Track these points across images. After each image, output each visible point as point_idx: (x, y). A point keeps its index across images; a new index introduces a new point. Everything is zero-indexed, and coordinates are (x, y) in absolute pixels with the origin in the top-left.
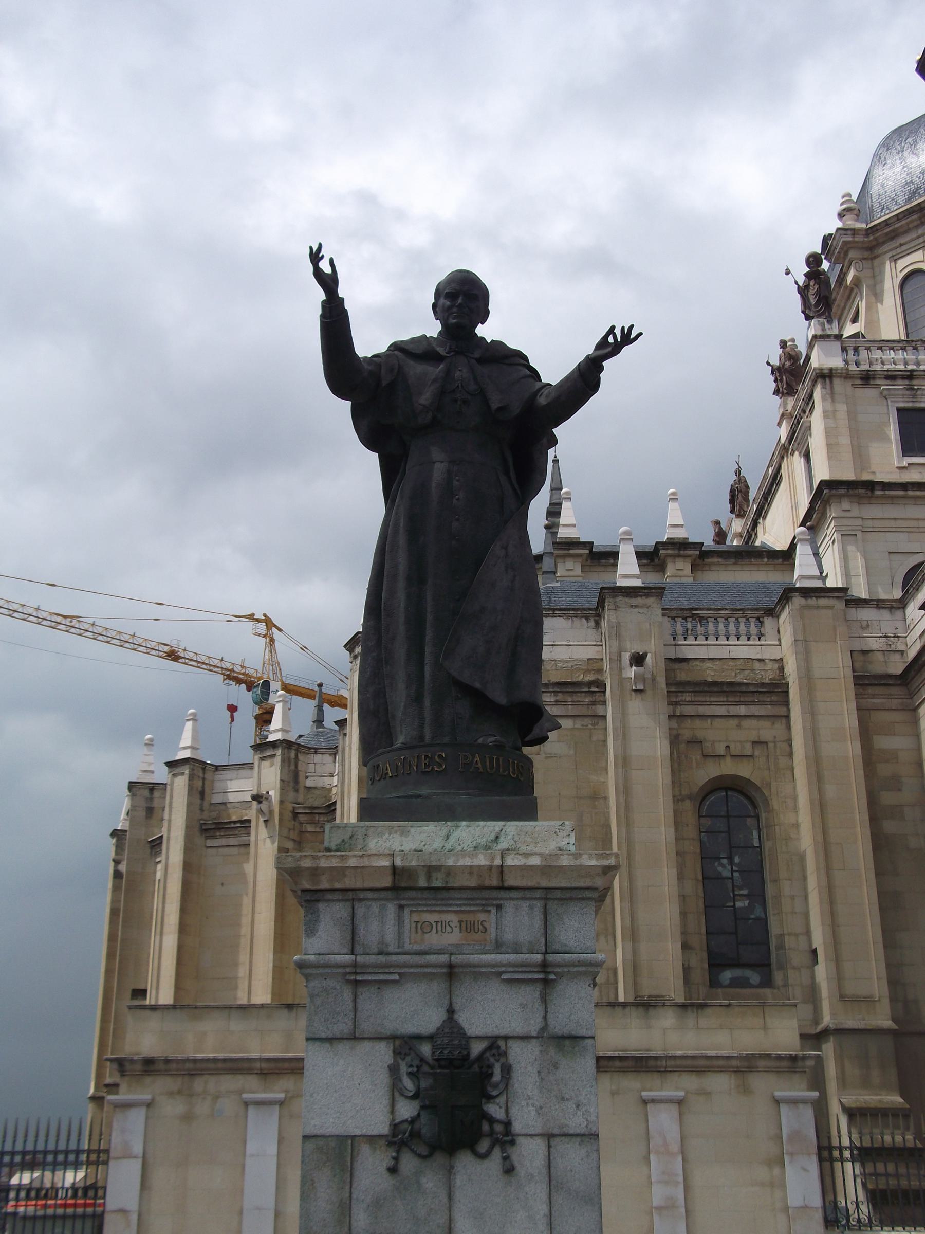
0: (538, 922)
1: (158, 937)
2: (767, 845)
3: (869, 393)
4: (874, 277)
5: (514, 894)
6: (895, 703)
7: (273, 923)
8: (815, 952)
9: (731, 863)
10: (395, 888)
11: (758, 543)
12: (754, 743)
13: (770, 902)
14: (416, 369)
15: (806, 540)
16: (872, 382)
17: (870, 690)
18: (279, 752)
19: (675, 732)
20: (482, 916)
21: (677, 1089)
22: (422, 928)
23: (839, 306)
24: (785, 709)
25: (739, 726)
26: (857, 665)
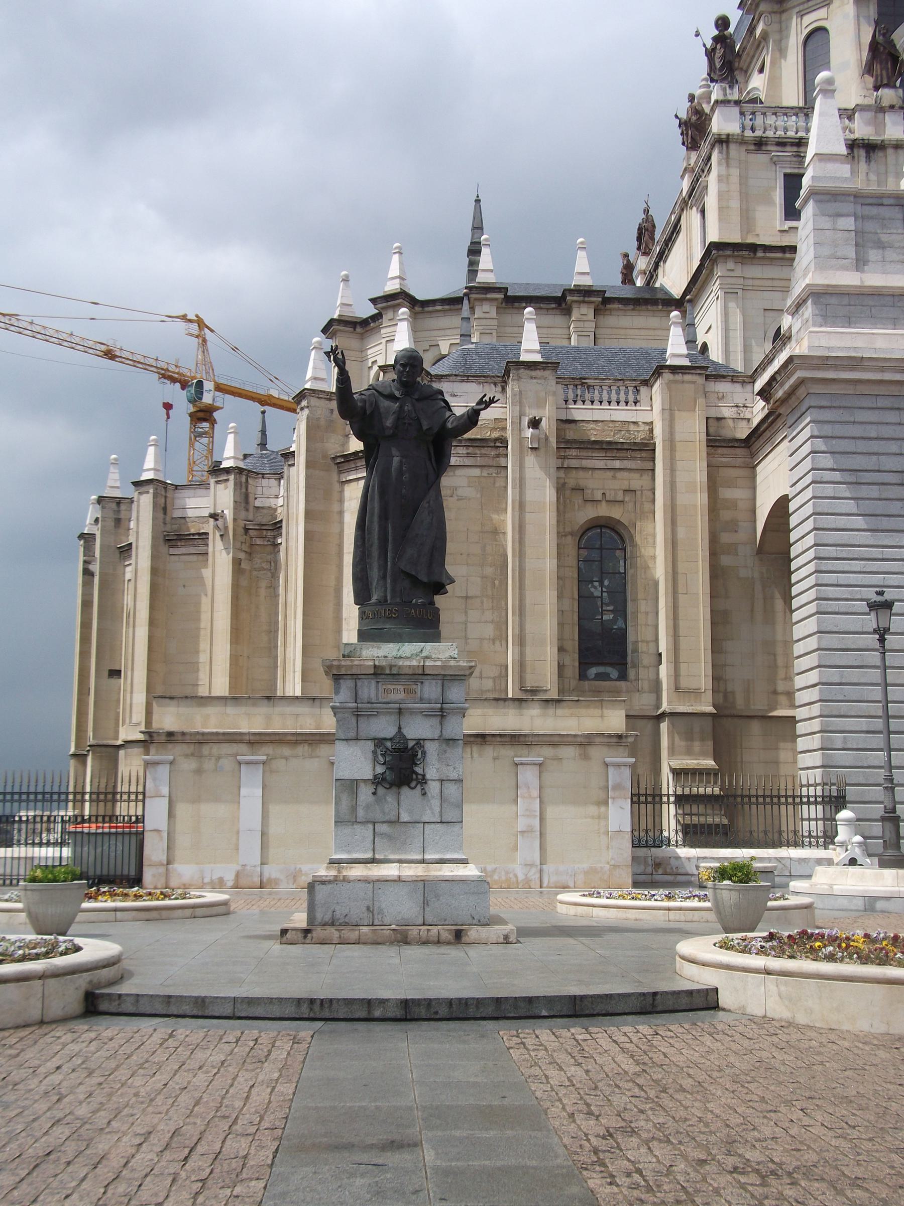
0: (439, 689)
1: (131, 629)
2: (630, 572)
3: (761, 158)
4: (781, 31)
5: (429, 677)
6: (739, 461)
7: (229, 620)
8: (660, 655)
9: (602, 585)
10: (375, 674)
11: (657, 285)
12: (625, 490)
13: (629, 616)
14: (385, 403)
15: (679, 323)
16: (764, 148)
17: (720, 451)
18: (232, 477)
19: (562, 481)
20: (414, 687)
21: (539, 756)
22: (387, 691)
23: (748, 54)
24: (652, 464)
25: (614, 477)
26: (711, 430)
